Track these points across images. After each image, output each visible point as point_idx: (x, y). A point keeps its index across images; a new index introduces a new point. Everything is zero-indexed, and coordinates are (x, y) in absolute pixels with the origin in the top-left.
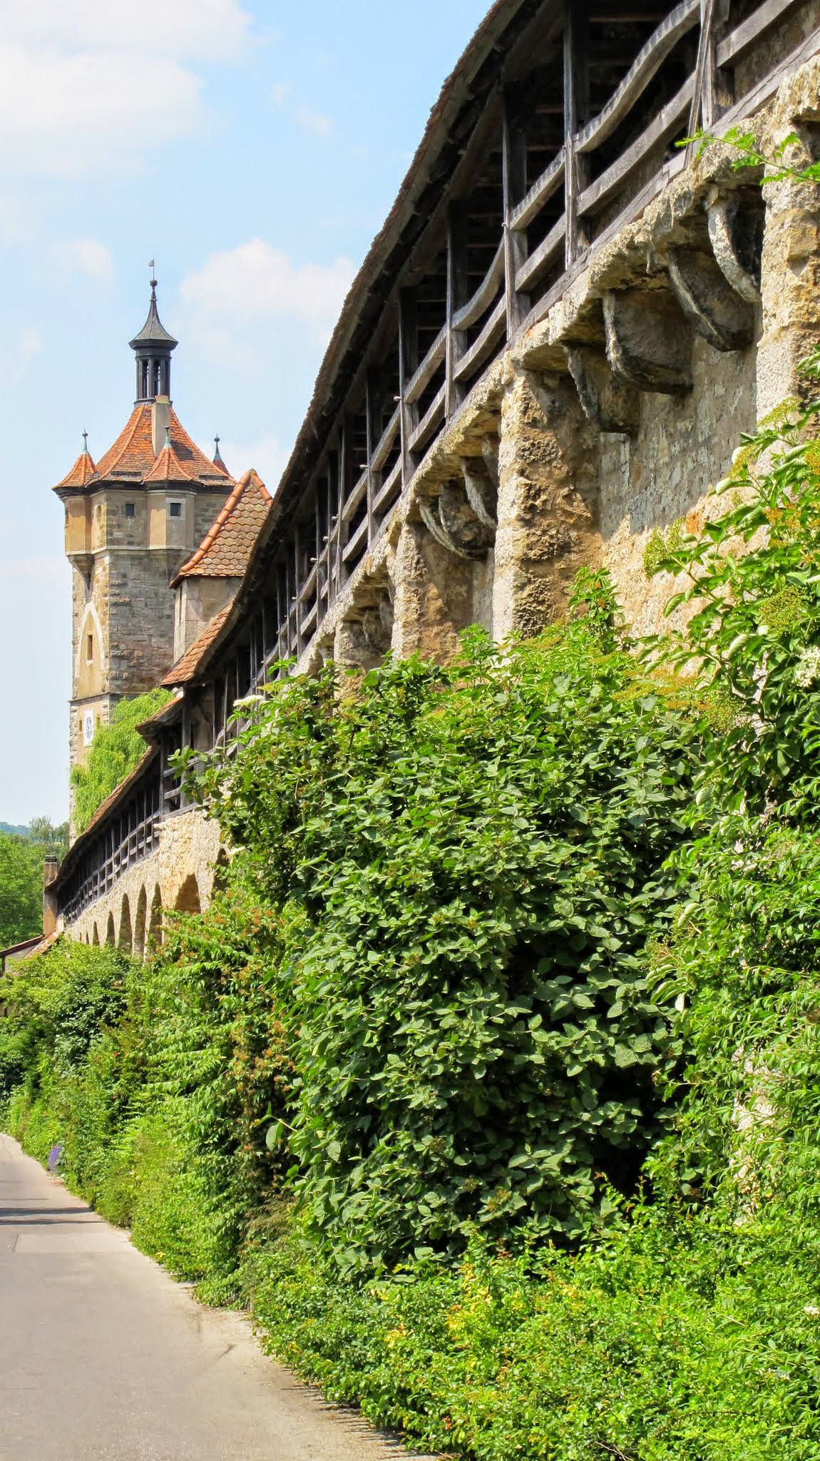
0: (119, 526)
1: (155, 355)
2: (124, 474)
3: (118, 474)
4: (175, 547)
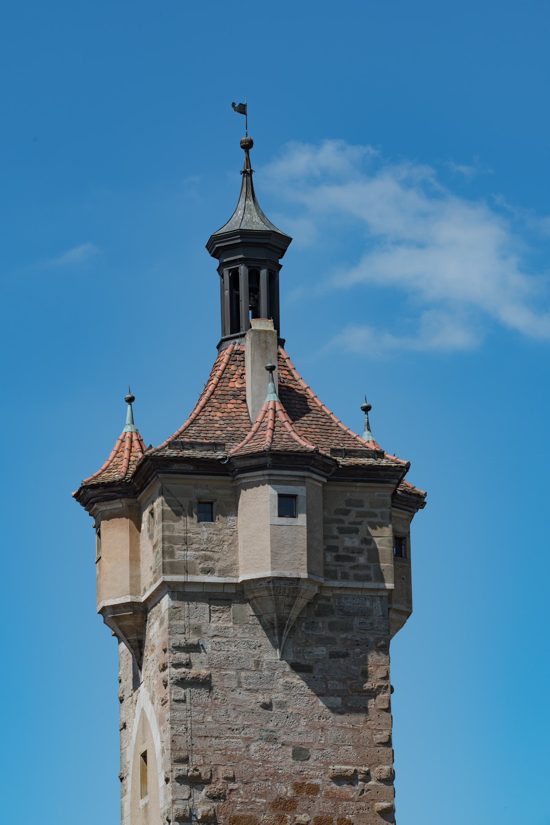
0: (186, 542)
1: (252, 265)
2: (192, 445)
3: (183, 446)
4: (288, 573)
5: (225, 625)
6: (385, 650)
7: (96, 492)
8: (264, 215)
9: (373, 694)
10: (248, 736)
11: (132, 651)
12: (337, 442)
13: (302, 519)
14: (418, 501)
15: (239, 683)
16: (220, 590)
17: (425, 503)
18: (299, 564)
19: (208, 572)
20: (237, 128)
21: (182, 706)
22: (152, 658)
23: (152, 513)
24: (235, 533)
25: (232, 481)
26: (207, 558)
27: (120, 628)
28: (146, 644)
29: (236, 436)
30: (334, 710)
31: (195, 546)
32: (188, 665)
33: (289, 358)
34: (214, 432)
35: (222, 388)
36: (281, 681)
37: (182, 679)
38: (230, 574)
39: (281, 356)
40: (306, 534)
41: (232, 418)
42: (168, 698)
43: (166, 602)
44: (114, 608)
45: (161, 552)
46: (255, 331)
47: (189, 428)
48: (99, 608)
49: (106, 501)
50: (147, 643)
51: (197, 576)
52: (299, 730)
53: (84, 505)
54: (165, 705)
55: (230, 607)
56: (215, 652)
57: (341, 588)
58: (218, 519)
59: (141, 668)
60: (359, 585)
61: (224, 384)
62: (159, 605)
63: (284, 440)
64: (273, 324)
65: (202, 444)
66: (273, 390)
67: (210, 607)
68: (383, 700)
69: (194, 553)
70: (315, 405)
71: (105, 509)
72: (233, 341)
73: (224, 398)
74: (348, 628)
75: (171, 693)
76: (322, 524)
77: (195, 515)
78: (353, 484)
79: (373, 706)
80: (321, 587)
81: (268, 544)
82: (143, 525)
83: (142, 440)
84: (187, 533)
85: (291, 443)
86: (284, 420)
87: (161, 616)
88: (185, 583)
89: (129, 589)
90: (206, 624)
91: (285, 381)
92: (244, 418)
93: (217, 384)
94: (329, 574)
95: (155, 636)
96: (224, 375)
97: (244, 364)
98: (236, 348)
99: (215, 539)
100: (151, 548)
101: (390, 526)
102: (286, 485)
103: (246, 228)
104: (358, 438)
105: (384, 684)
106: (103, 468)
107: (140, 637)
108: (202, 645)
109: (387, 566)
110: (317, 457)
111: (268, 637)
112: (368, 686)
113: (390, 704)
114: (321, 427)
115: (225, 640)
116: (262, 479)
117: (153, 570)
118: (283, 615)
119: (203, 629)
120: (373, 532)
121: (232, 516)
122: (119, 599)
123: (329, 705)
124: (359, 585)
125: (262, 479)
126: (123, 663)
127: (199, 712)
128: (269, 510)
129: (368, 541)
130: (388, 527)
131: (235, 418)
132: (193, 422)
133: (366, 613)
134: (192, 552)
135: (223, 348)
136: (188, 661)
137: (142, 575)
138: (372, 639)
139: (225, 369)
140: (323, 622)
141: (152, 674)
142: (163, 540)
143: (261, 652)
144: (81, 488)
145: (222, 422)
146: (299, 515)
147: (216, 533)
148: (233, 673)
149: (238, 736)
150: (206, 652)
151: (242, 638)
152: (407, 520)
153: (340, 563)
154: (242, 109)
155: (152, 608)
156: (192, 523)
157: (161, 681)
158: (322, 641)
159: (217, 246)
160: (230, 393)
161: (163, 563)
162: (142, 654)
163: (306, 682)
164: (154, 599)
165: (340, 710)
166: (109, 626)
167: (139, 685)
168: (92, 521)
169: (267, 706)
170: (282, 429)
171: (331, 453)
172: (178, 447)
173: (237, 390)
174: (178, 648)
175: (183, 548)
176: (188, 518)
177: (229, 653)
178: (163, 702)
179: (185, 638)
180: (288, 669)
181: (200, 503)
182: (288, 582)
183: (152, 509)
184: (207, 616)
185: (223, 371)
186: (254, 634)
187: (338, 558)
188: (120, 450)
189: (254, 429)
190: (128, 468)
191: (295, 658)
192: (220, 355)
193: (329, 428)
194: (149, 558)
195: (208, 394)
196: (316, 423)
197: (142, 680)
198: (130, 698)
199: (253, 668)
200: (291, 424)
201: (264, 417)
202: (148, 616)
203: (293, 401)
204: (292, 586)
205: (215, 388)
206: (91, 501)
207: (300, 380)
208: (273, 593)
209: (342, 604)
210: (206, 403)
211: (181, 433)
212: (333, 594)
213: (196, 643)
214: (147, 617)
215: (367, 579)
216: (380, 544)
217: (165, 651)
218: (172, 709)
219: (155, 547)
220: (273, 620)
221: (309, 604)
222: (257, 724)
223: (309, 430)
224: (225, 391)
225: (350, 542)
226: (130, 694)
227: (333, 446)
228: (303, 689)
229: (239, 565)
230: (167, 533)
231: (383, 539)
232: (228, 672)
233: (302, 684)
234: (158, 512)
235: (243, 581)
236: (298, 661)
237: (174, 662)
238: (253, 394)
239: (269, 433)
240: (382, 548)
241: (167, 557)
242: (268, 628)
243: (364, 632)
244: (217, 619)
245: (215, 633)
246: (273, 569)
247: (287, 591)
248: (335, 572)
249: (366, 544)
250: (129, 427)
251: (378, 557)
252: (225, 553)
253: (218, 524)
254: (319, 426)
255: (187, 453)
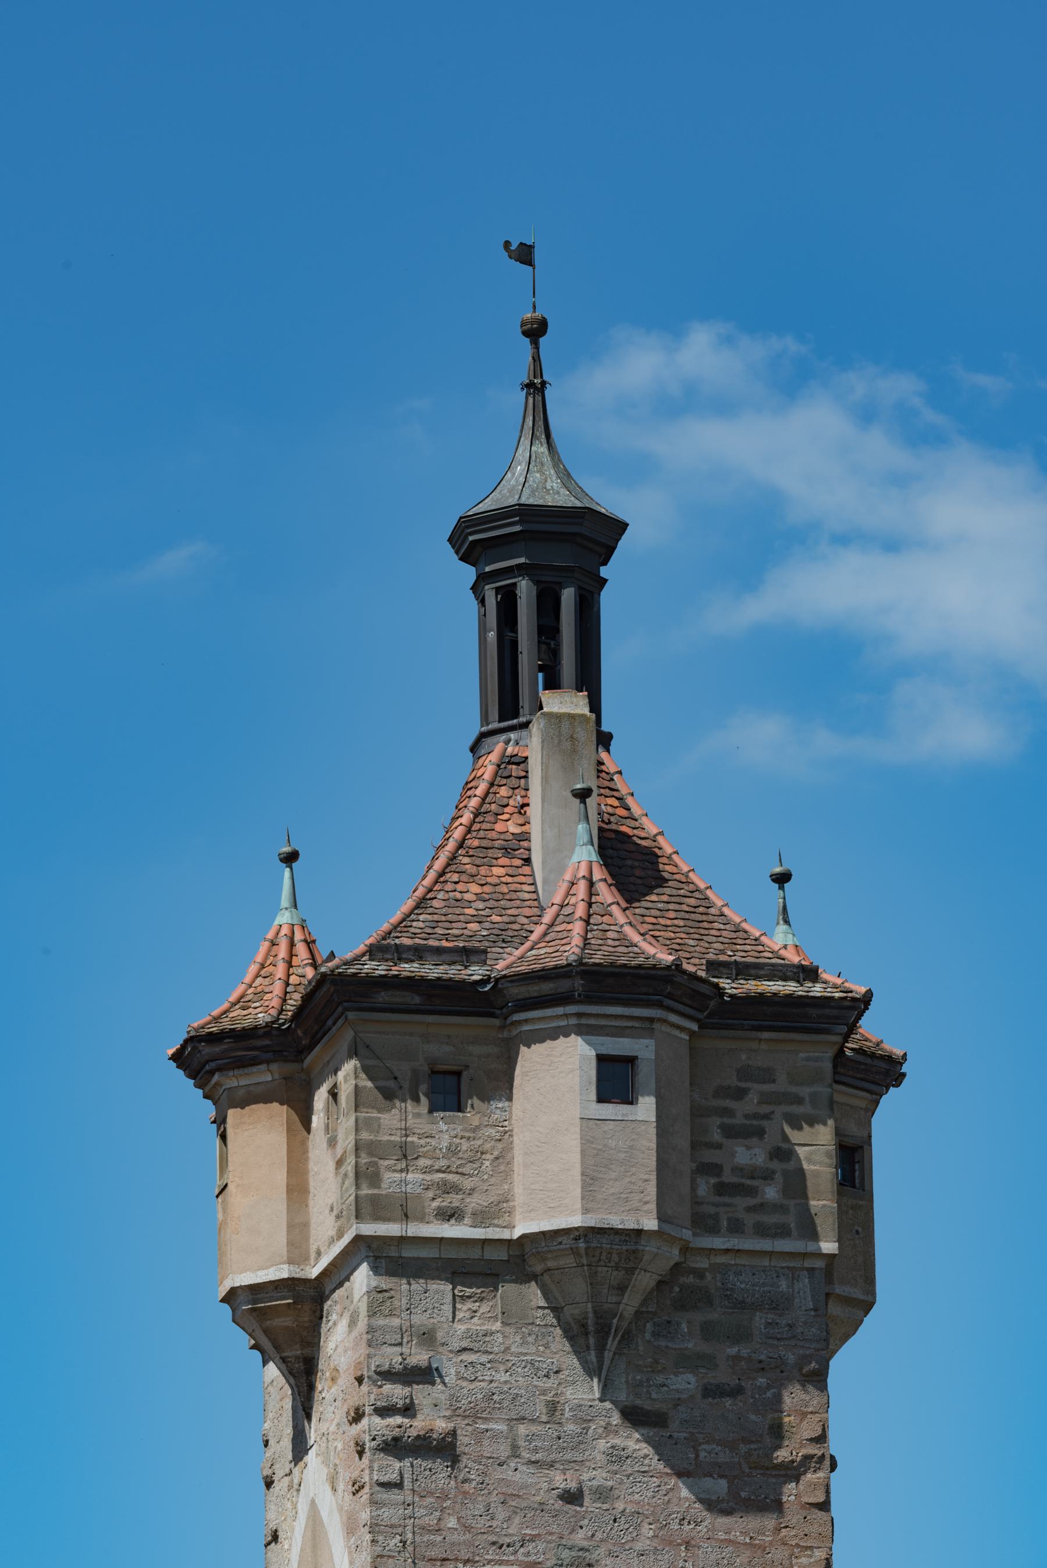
0: (405, 1153)
1: (544, 579)
2: (419, 953)
3: (400, 953)
4: (615, 1221)
5: (484, 1328)
6: (819, 1381)
7: (217, 1049)
8: (569, 475)
9: (793, 1472)
10: (533, 1558)
11: (292, 1381)
12: (721, 947)
13: (646, 1108)
14: (888, 1071)
15: (515, 1447)
16: (475, 1253)
17: (904, 1075)
18: (640, 1201)
19: (451, 1216)
20: (514, 295)
21: (395, 1496)
22: (333, 1397)
23: (334, 1094)
24: (506, 1136)
25: (502, 1028)
26: (448, 1188)
27: (266, 1332)
28: (320, 1367)
29: (510, 933)
30: (713, 1505)
31: (422, 1162)
32: (409, 1410)
33: (620, 772)
34: (464, 925)
35: (482, 834)
36: (602, 1445)
37: (396, 1439)
38: (496, 1222)
39: (603, 768)
40: (654, 1138)
41: (501, 897)
42: (366, 1479)
43: (362, 1278)
44: (255, 1290)
45: (351, 1175)
46: (550, 715)
47: (413, 917)
48: (223, 1291)
49: (239, 1067)
50: (322, 1364)
51: (427, 1226)
52: (639, 1546)
53: (190, 1076)
54: (360, 1494)
55: (497, 1290)
56: (464, 1384)
57: (727, 1251)
58: (472, 1106)
59: (309, 1417)
60: (765, 1245)
61: (484, 826)
62: (347, 1284)
63: (610, 942)
64: (587, 700)
65: (439, 951)
66: (586, 838)
67: (453, 1289)
68: (814, 1486)
69: (421, 1176)
70: (675, 870)
71: (236, 1084)
72: (503, 737)
73: (484, 854)
74: (741, 1335)
75: (371, 1468)
76: (688, 1118)
77: (423, 1098)
78: (753, 1034)
79: (793, 1497)
80: (686, 1249)
81: (576, 1158)
82: (315, 1118)
83: (314, 942)
84: (407, 1136)
85: (625, 950)
86: (610, 900)
87: (352, 1308)
88: (402, 1240)
89: (284, 1251)
90: (445, 1326)
91: (612, 819)
92: (527, 896)
93: (471, 825)
94: (704, 1223)
95: (339, 1350)
96: (485, 808)
97: (527, 783)
98: (510, 750)
99: (464, 1148)
100: (332, 1165)
101: (831, 1122)
102: (613, 1036)
103: (531, 501)
104: (763, 939)
105: (816, 1452)
106: (233, 998)
107: (307, 1351)
108: (437, 1369)
109: (824, 1206)
110: (678, 979)
111: (576, 1353)
112: (782, 1455)
113: (828, 1492)
114: (687, 916)
115: (484, 1358)
116: (563, 1023)
117: (335, 1212)
118: (606, 1306)
119: (440, 1335)
120: (795, 1136)
121: (500, 1100)
122: (265, 1272)
123: (702, 1496)
124: (765, 1245)
125: (563, 1023)
126: (272, 1406)
127: (431, 1510)
128: (577, 1088)
129: (784, 1153)
130: (825, 1124)
131: (507, 897)
132: (422, 904)
133: (778, 1304)
134: (417, 1176)
135: (483, 752)
136: (408, 1401)
137: (312, 1221)
138: (791, 1358)
139: (487, 793)
140: (689, 1322)
141: (333, 1428)
142: (357, 1149)
143: (560, 1384)
144: (186, 1042)
145: (480, 905)
146: (640, 1099)
147: (467, 1134)
148: (502, 1427)
149: (512, 1558)
150: (445, 1384)
151: (522, 1354)
152: (866, 1110)
153: (726, 1199)
154: (525, 255)
155: (334, 1291)
156: (417, 1115)
157: (352, 1444)
158: (686, 1362)
159: (471, 538)
160: (497, 844)
161: (357, 1197)
162: (311, 1387)
163: (653, 1447)
164: (338, 1273)
165: (724, 1505)
166: (243, 1328)
167: (306, 1451)
168: (209, 1109)
169: (572, 1497)
170: (606, 919)
171: (707, 970)
172: (389, 956)
173: (511, 837)
174: (387, 1375)
175: (398, 1167)
176: (410, 1105)
177: (493, 1385)
178: (356, 1487)
179: (401, 1354)
180: (616, 1419)
181: (433, 1072)
182: (617, 1238)
183: (335, 1086)
184: (448, 1308)
185: (484, 799)
186: (547, 1346)
187: (722, 1189)
188: (268, 962)
189: (547, 919)
190: (285, 1000)
191: (631, 1398)
192: (477, 767)
193: (704, 918)
194: (328, 1186)
195: (451, 845)
196: (677, 907)
197: (311, 1442)
198: (287, 1479)
199: (544, 1418)
200: (624, 910)
201: (568, 894)
202: (326, 1307)
203: (629, 862)
204: (624, 1248)
205: (466, 835)
206: (207, 1067)
207: (644, 819)
208: (585, 1261)
209: (729, 1285)
210: (448, 865)
211: (395, 927)
212: (710, 1264)
213: (425, 1364)
214: (322, 1310)
215: (782, 1232)
216: (810, 1161)
217: (360, 1380)
218: (373, 1502)
219: (339, 1163)
220: (586, 1318)
221: (660, 1283)
222: (551, 1534)
223: (662, 921)
224: (487, 841)
225: (747, 1155)
226: (287, 1471)
227: (711, 956)
228: (647, 1461)
229: (516, 1203)
230: (365, 1136)
231: (815, 1149)
232: (492, 1426)
233: (646, 1451)
234: (346, 1092)
235: (523, 1237)
236: (638, 1402)
237: (379, 1403)
238: (544, 847)
239: (578, 927)
240: (812, 1167)
241: (364, 1186)
242: (577, 1334)
243: (775, 1342)
244: (468, 1315)
245: (465, 1344)
246: (586, 1211)
247: (615, 1258)
248: (716, 1217)
249: (781, 1160)
250: (287, 914)
251: (805, 1187)
252: (485, 1177)
253: (471, 1116)
254: (682, 915)
255: (408, 968)
